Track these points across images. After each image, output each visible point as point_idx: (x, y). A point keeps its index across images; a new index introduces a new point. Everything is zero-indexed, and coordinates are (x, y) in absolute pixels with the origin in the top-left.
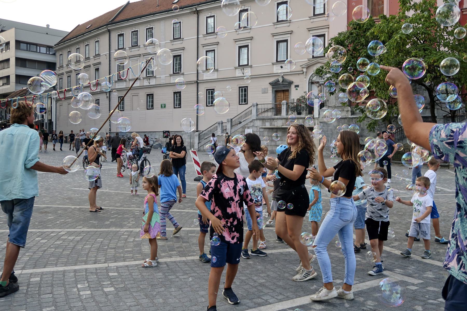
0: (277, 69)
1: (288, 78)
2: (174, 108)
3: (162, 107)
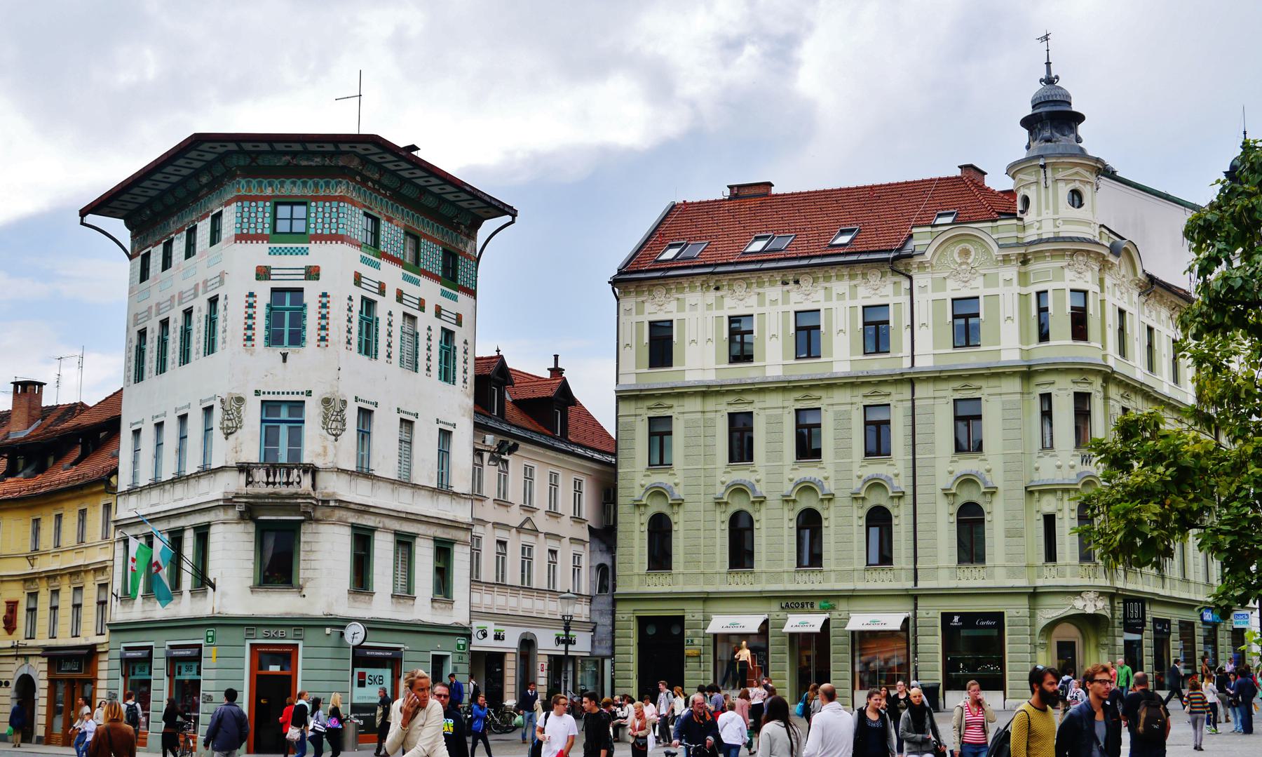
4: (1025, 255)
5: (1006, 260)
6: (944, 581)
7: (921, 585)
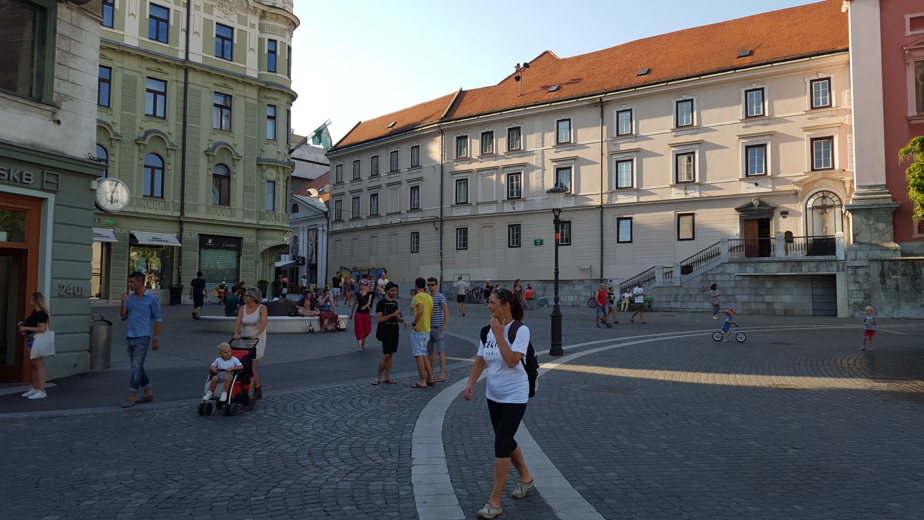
0: (748, 188)
1: (771, 202)
2: (509, 247)
3: (536, 244)
4: (264, 11)
5: (255, 10)
6: (201, 214)
7: (186, 215)
